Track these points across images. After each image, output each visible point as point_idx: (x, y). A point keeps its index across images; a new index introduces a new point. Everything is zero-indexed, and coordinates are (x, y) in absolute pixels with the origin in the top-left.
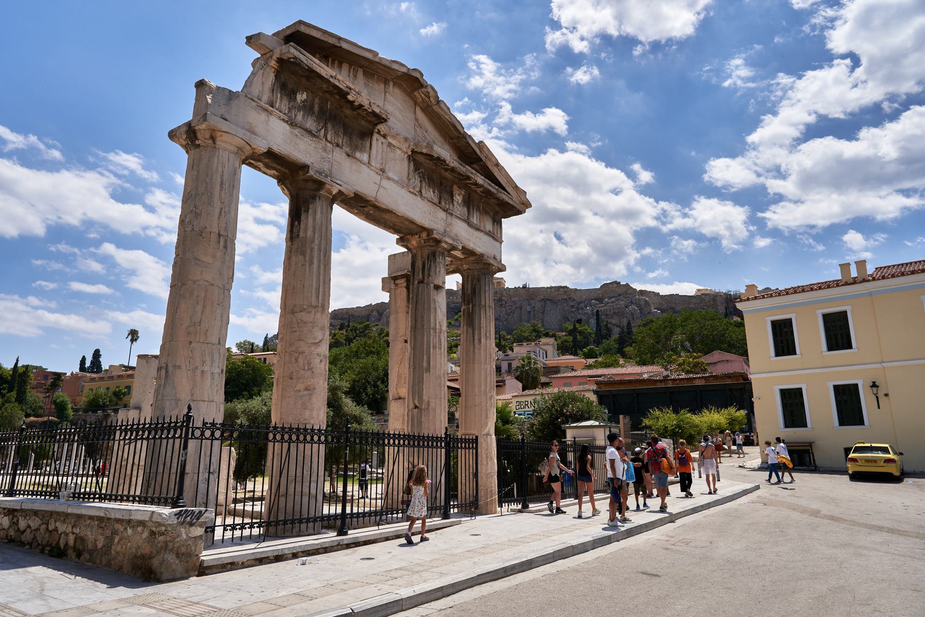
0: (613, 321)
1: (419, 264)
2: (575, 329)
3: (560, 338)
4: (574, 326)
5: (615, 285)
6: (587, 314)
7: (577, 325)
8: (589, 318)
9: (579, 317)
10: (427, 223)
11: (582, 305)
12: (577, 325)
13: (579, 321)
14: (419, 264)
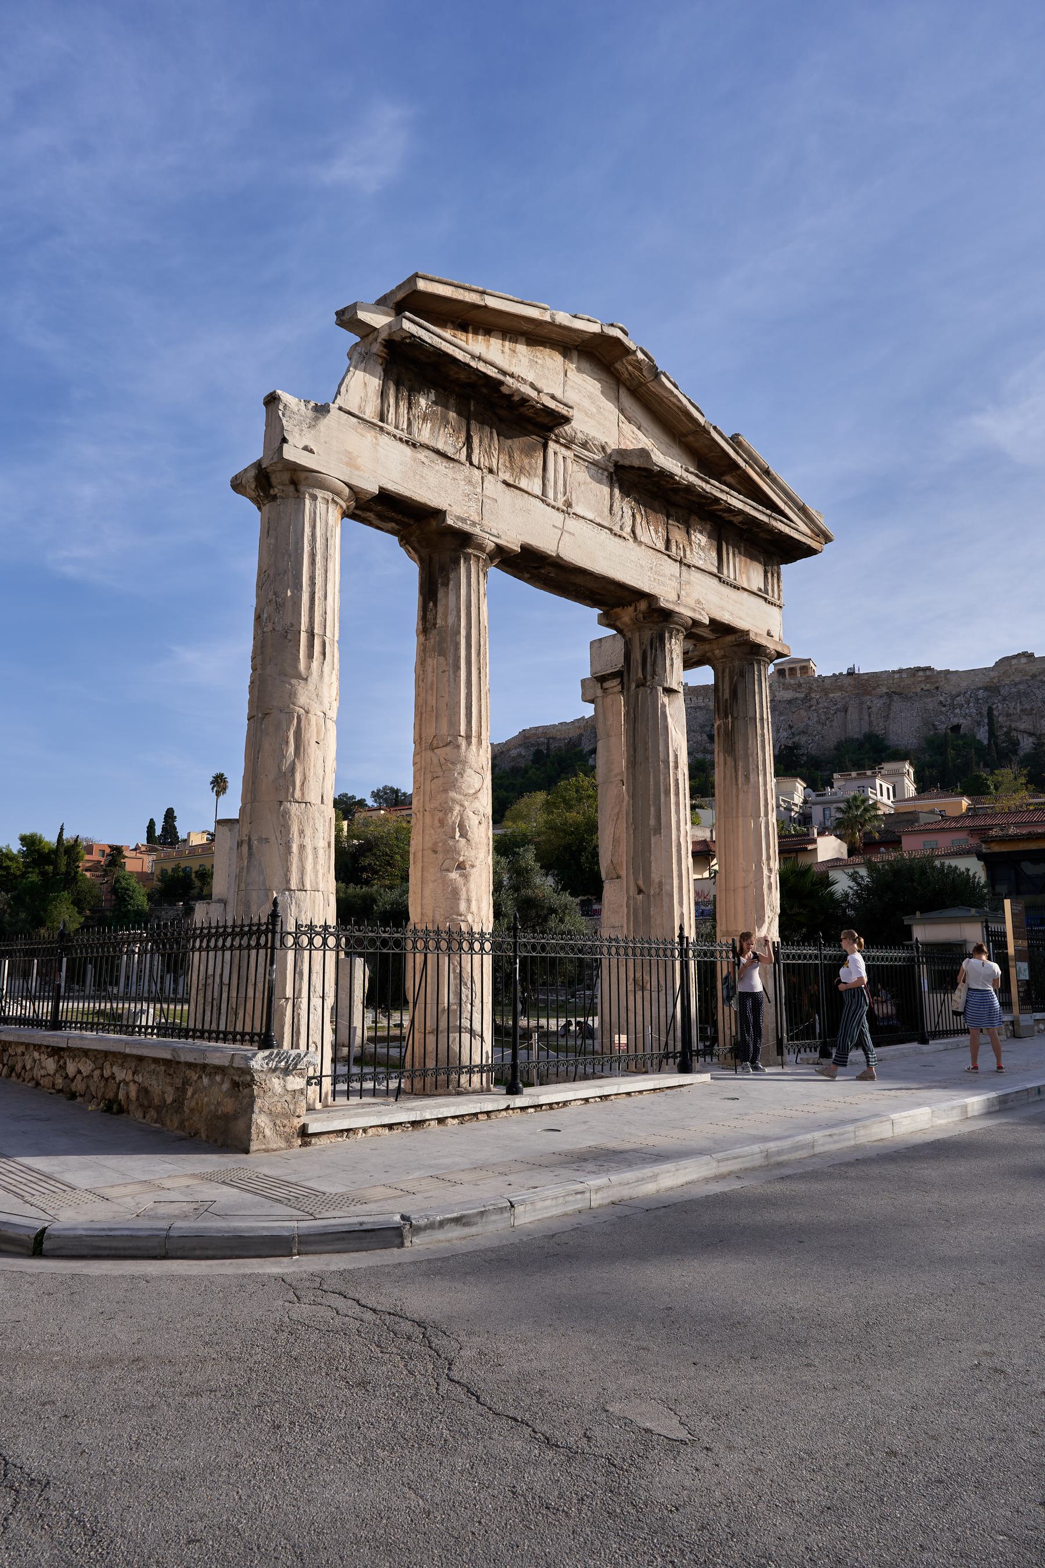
0: (1022, 727)
1: (637, 655)
5: (1024, 660)
9: (955, 721)
10: (644, 585)
11: (960, 700)
14: (637, 655)
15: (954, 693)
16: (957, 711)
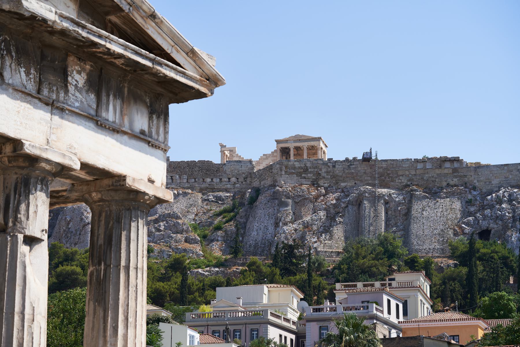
2: (472, 250)
3: (440, 269)
4: (472, 243)
6: (501, 218)
7: (479, 243)
8: (506, 228)
9: (484, 224)
12: (479, 243)
13: (485, 234)
15: (484, 190)
16: (488, 212)
